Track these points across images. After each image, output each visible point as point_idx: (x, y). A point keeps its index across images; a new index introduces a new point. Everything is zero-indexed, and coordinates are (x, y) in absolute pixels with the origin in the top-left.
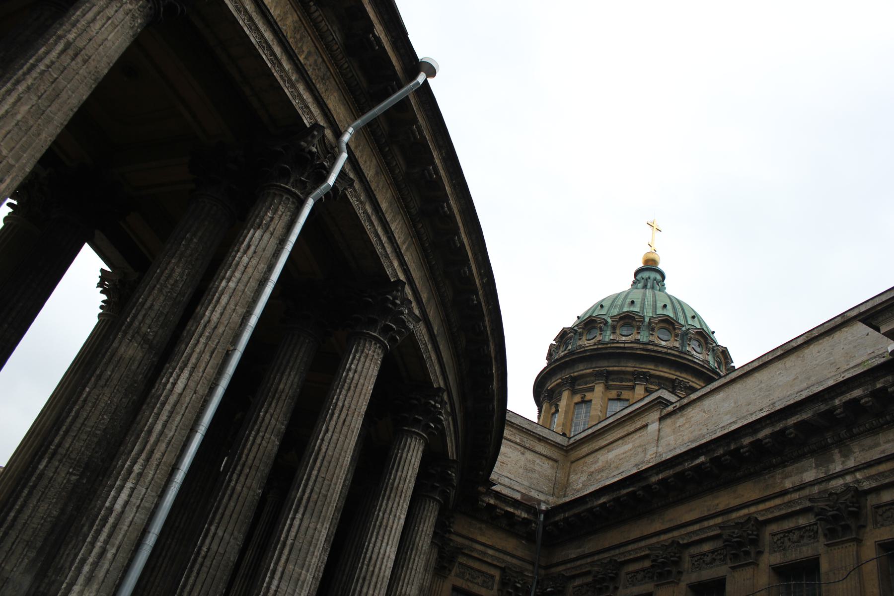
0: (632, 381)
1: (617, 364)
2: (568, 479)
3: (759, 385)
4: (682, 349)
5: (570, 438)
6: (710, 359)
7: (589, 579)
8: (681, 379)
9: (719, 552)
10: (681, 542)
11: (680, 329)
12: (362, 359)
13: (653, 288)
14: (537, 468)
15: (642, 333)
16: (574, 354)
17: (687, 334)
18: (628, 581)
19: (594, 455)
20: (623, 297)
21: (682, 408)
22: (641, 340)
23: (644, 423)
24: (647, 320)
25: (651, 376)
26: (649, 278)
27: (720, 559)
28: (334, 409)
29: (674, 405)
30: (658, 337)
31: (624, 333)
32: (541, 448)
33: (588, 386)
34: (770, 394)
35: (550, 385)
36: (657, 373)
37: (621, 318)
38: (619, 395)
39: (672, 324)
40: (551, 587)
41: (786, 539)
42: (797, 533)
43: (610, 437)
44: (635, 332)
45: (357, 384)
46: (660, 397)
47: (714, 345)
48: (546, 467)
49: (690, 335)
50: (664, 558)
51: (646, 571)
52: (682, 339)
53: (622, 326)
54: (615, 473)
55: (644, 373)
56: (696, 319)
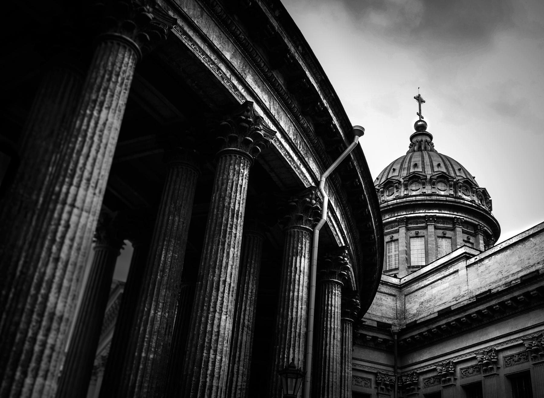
0: (425, 223)
3: (534, 246)
4: (456, 195)
5: (401, 279)
6: (475, 198)
7: (435, 374)
10: (496, 349)
11: (453, 181)
12: (333, 297)
13: (425, 149)
14: (384, 303)
15: (427, 187)
17: (458, 184)
18: (463, 374)
22: (427, 193)
23: (455, 270)
24: (429, 177)
26: (422, 141)
27: (524, 358)
28: (327, 330)
29: (475, 257)
30: (438, 188)
31: (414, 188)
33: (394, 229)
37: (410, 179)
39: (447, 178)
43: (431, 279)
44: (421, 187)
45: (335, 313)
47: (477, 188)
52: (455, 188)
53: (412, 184)
54: (440, 303)
56: (461, 170)
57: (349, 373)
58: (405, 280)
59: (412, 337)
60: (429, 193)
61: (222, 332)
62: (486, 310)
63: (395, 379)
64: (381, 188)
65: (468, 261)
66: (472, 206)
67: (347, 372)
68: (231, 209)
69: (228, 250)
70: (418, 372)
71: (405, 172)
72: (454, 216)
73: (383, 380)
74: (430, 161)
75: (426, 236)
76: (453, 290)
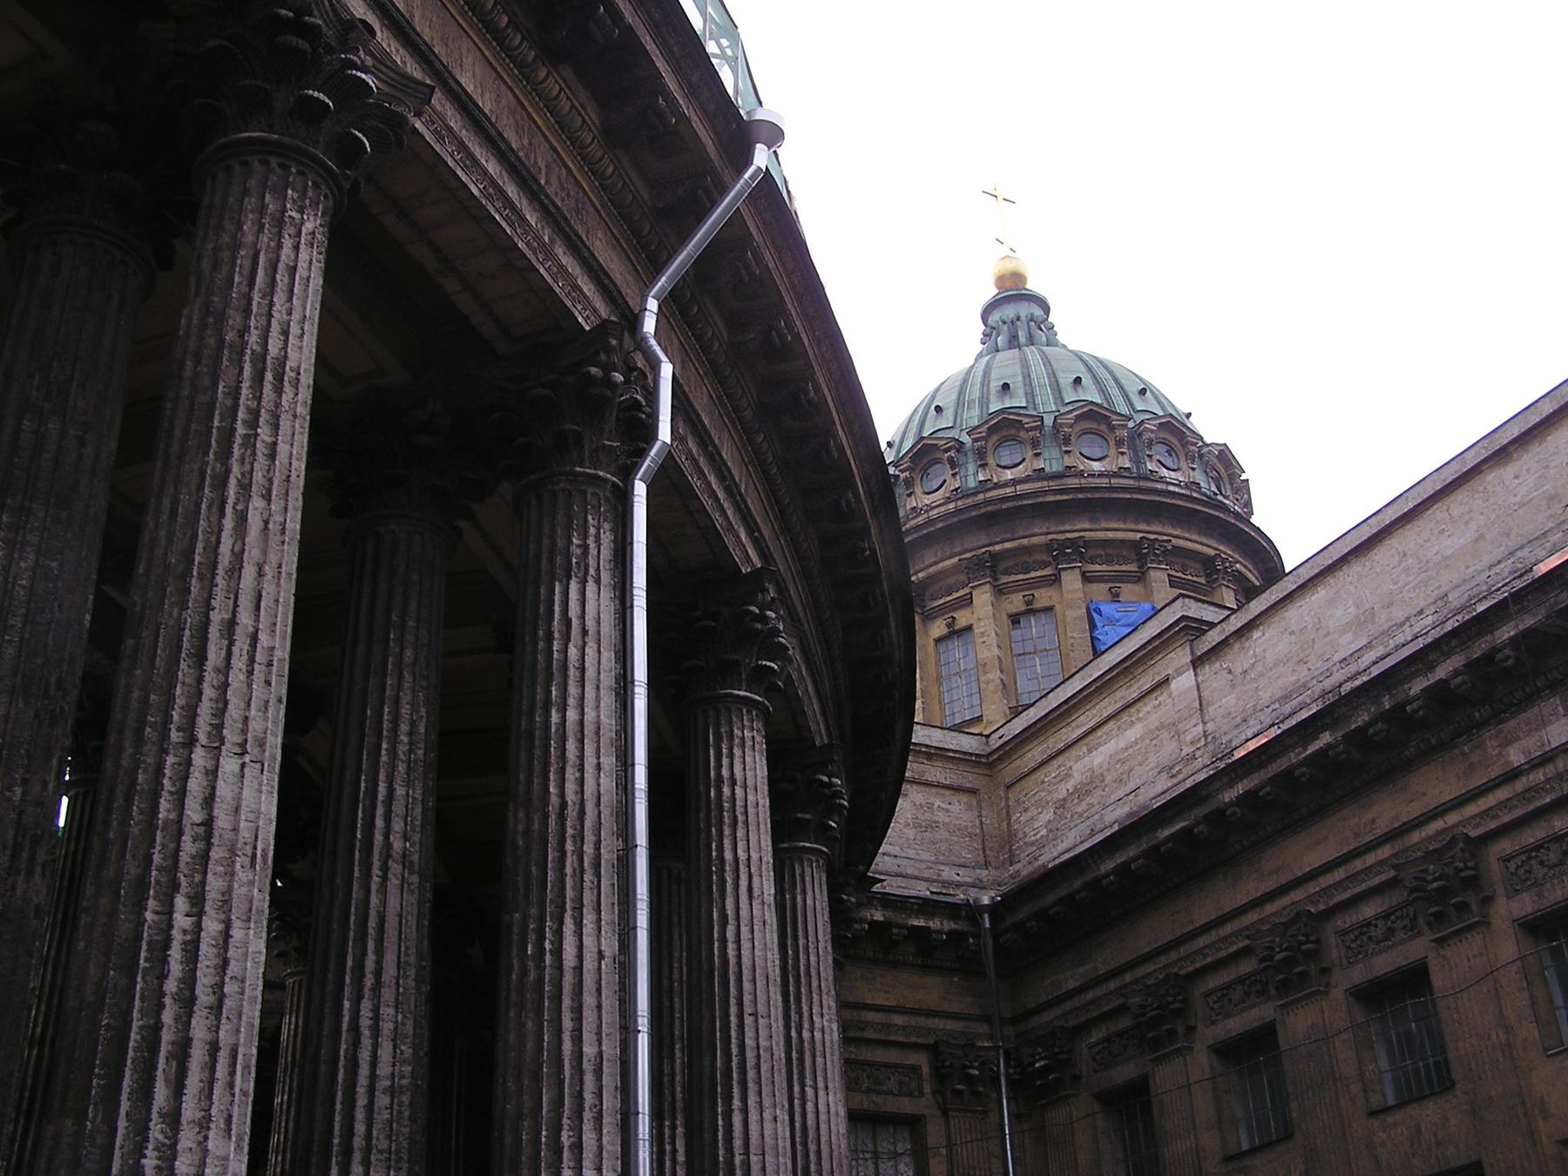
0: (1050, 564)
1: (1009, 536)
2: (1009, 824)
3: (1400, 562)
4: (1138, 469)
5: (988, 736)
6: (1199, 477)
7: (1124, 1022)
9: (1399, 913)
10: (1312, 910)
12: (737, 752)
13: (1031, 340)
14: (941, 817)
15: (1046, 455)
17: (1140, 435)
18: (1212, 1008)
19: (1055, 763)
20: (979, 379)
22: (1047, 470)
23: (1158, 678)
24: (1049, 421)
25: (1088, 544)
27: (1404, 927)
28: (722, 870)
33: (956, 595)
34: (1430, 578)
36: (1100, 535)
37: (992, 430)
38: (1029, 603)
40: (1041, 1059)
41: (1533, 862)
42: (1554, 847)
43: (1085, 720)
47: (1200, 444)
49: (1146, 436)
50: (1286, 949)
51: (1247, 982)
52: (1133, 447)
54: (1120, 793)
55: (1073, 543)
56: (1148, 393)
57: (827, 1030)
58: (1001, 738)
60: (1054, 470)
61: (222, 822)
62: (1268, 788)
64: (902, 471)
66: (1190, 499)
67: (817, 1026)
68: (249, 351)
69: (239, 507)
71: (976, 412)
72: (1140, 535)
74: (1048, 374)
75: (1058, 609)
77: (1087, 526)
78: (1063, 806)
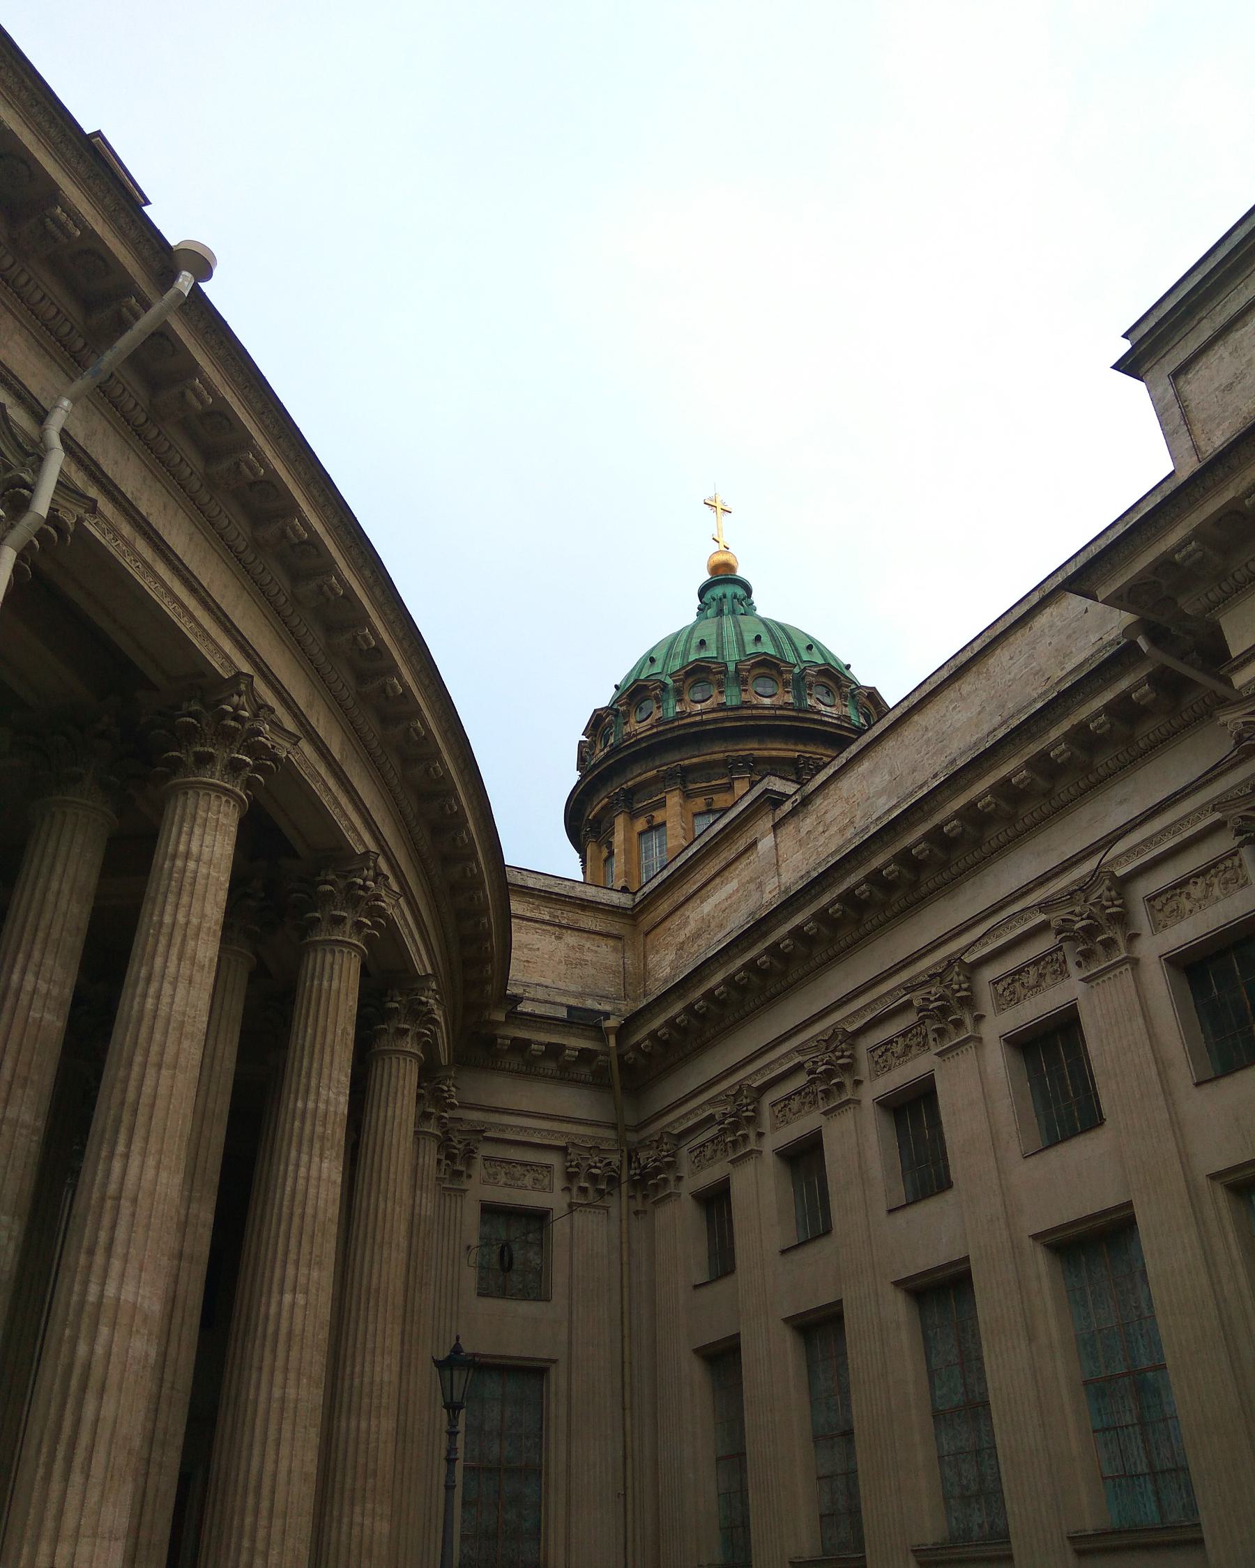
1: (696, 753)
4: (800, 704)
5: (635, 894)
6: (850, 711)
8: (808, 755)
9: (914, 1032)
11: (791, 672)
12: (197, 831)
13: (733, 612)
14: (589, 956)
15: (728, 692)
16: (621, 751)
17: (803, 678)
19: (678, 913)
20: (684, 637)
21: (806, 801)
22: (728, 704)
23: (749, 841)
24: (731, 667)
25: (757, 760)
26: (725, 596)
27: (918, 1044)
29: (793, 799)
30: (756, 693)
31: (698, 697)
32: (588, 921)
34: (945, 747)
35: (592, 813)
36: (766, 753)
37: (688, 674)
38: (709, 804)
39: (776, 666)
41: (1017, 984)
42: (1032, 970)
43: (699, 878)
44: (715, 692)
45: (195, 878)
46: (766, 791)
47: (853, 686)
48: (604, 953)
51: (803, 1094)
53: (693, 687)
59: (653, 1035)
63: (621, 1161)
65: (778, 812)
70: (676, 1132)
72: (797, 754)
73: (584, 1164)
74: (736, 634)
76: (748, 896)
77: (756, 746)
78: (681, 948)
